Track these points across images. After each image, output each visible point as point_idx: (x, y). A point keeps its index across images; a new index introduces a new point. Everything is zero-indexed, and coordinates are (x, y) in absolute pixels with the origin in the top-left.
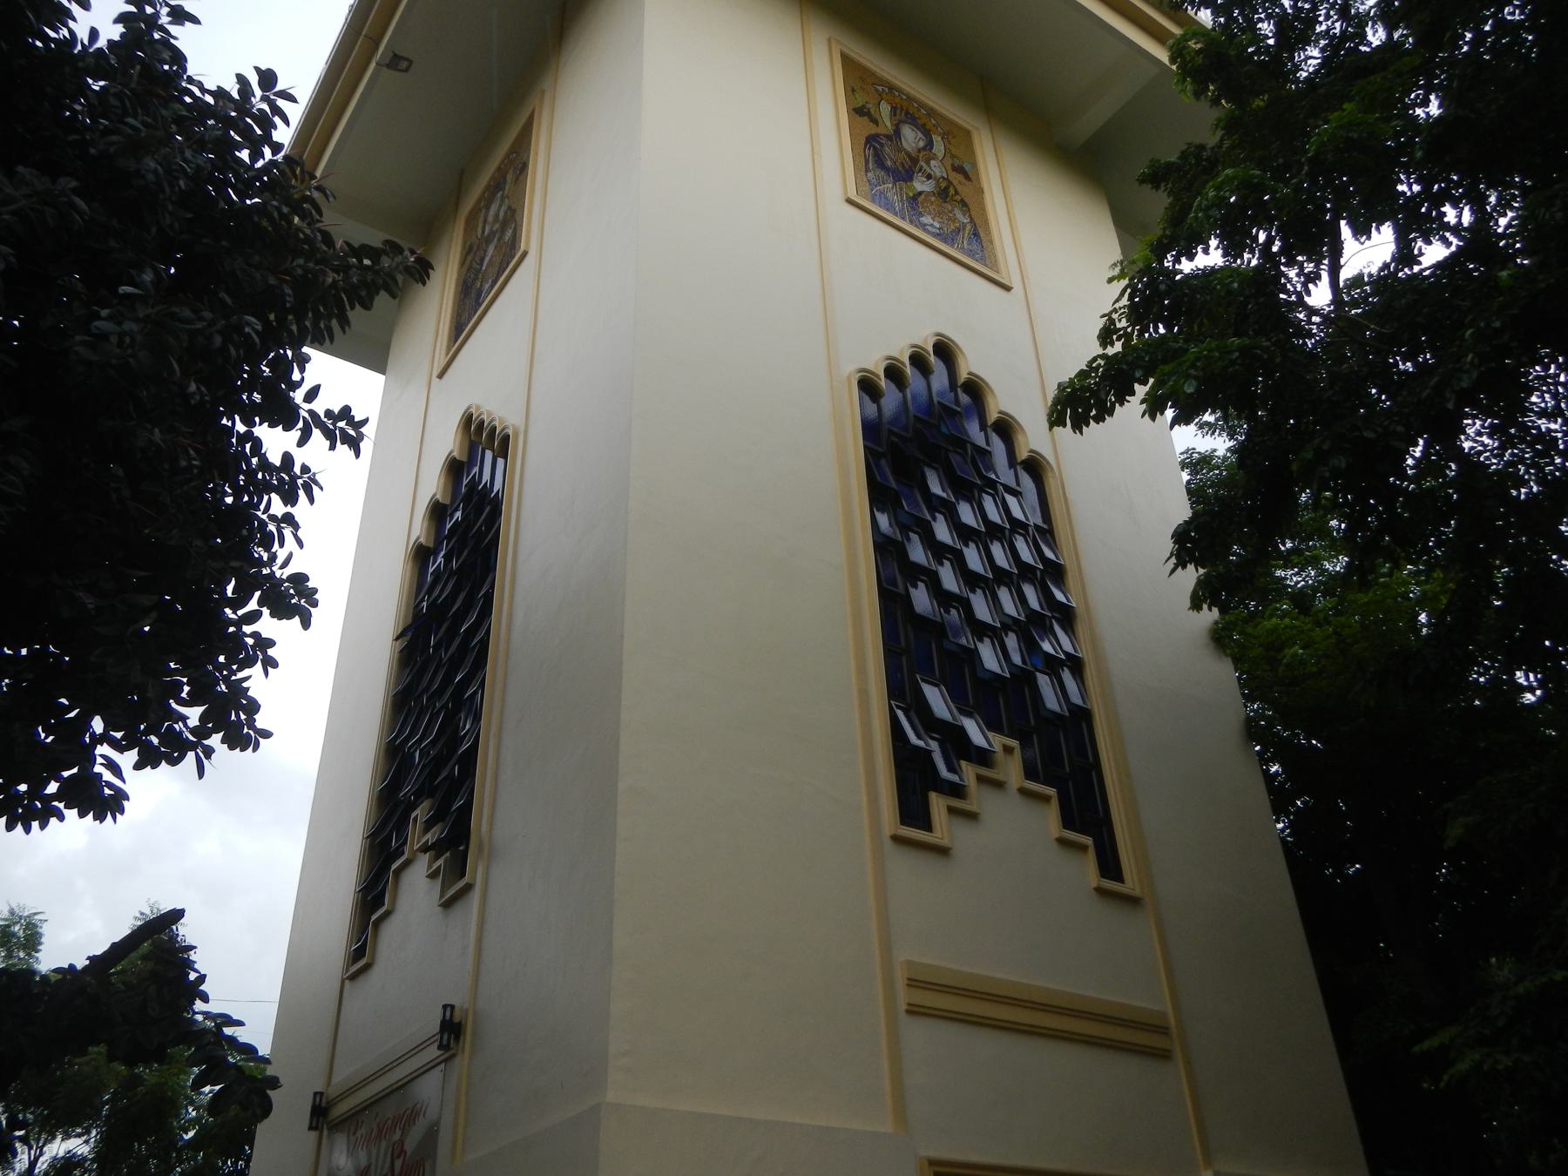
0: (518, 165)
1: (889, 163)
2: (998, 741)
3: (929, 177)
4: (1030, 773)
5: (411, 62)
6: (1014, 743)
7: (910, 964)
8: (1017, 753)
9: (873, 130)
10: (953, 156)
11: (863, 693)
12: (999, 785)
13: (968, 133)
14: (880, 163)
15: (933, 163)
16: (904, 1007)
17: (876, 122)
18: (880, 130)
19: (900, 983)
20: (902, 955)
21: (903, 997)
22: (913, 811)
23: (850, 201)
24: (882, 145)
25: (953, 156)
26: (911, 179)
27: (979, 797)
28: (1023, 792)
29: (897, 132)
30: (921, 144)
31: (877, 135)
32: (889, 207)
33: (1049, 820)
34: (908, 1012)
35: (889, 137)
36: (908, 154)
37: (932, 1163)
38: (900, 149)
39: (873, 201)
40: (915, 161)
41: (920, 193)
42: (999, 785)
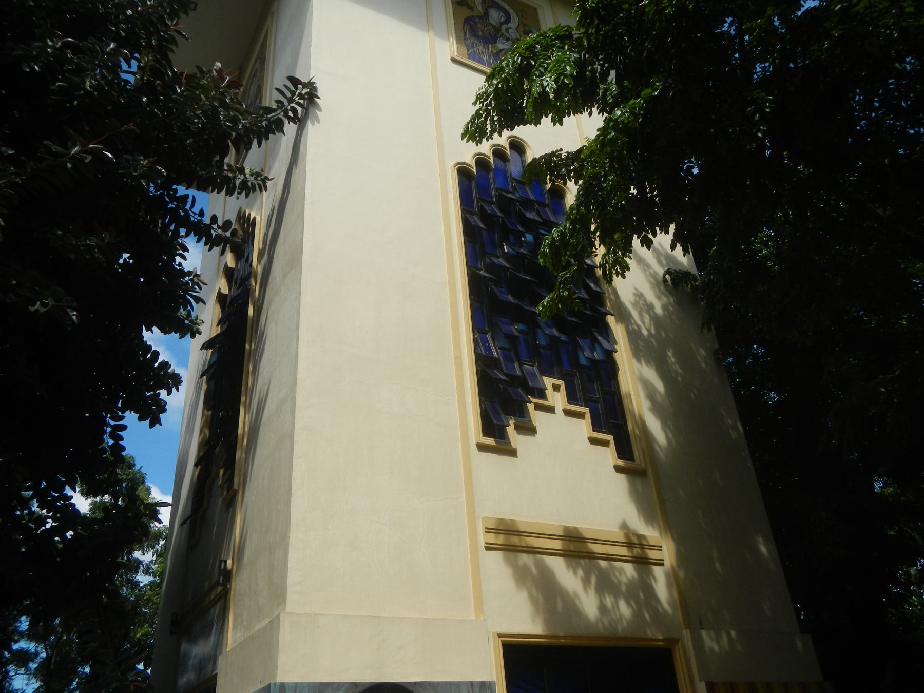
0: (262, 59)
1: (480, 33)
2: (548, 382)
3: (508, 39)
4: (571, 398)
5: (196, 4)
6: (561, 383)
7: (484, 519)
8: (563, 388)
9: (469, 13)
10: (524, 25)
11: (459, 359)
12: (551, 410)
14: (474, 34)
15: (510, 31)
16: (483, 545)
17: (471, 8)
18: (475, 13)
21: (483, 538)
22: (492, 427)
23: (454, 60)
24: (475, 22)
25: (524, 25)
26: (495, 42)
27: (538, 418)
28: (567, 413)
29: (486, 13)
30: (503, 19)
31: (473, 17)
32: (480, 61)
33: (583, 427)
34: (487, 549)
35: (480, 17)
36: (494, 27)
37: (500, 636)
38: (489, 24)
39: (469, 58)
40: (497, 30)
41: (502, 50)
42: (551, 410)
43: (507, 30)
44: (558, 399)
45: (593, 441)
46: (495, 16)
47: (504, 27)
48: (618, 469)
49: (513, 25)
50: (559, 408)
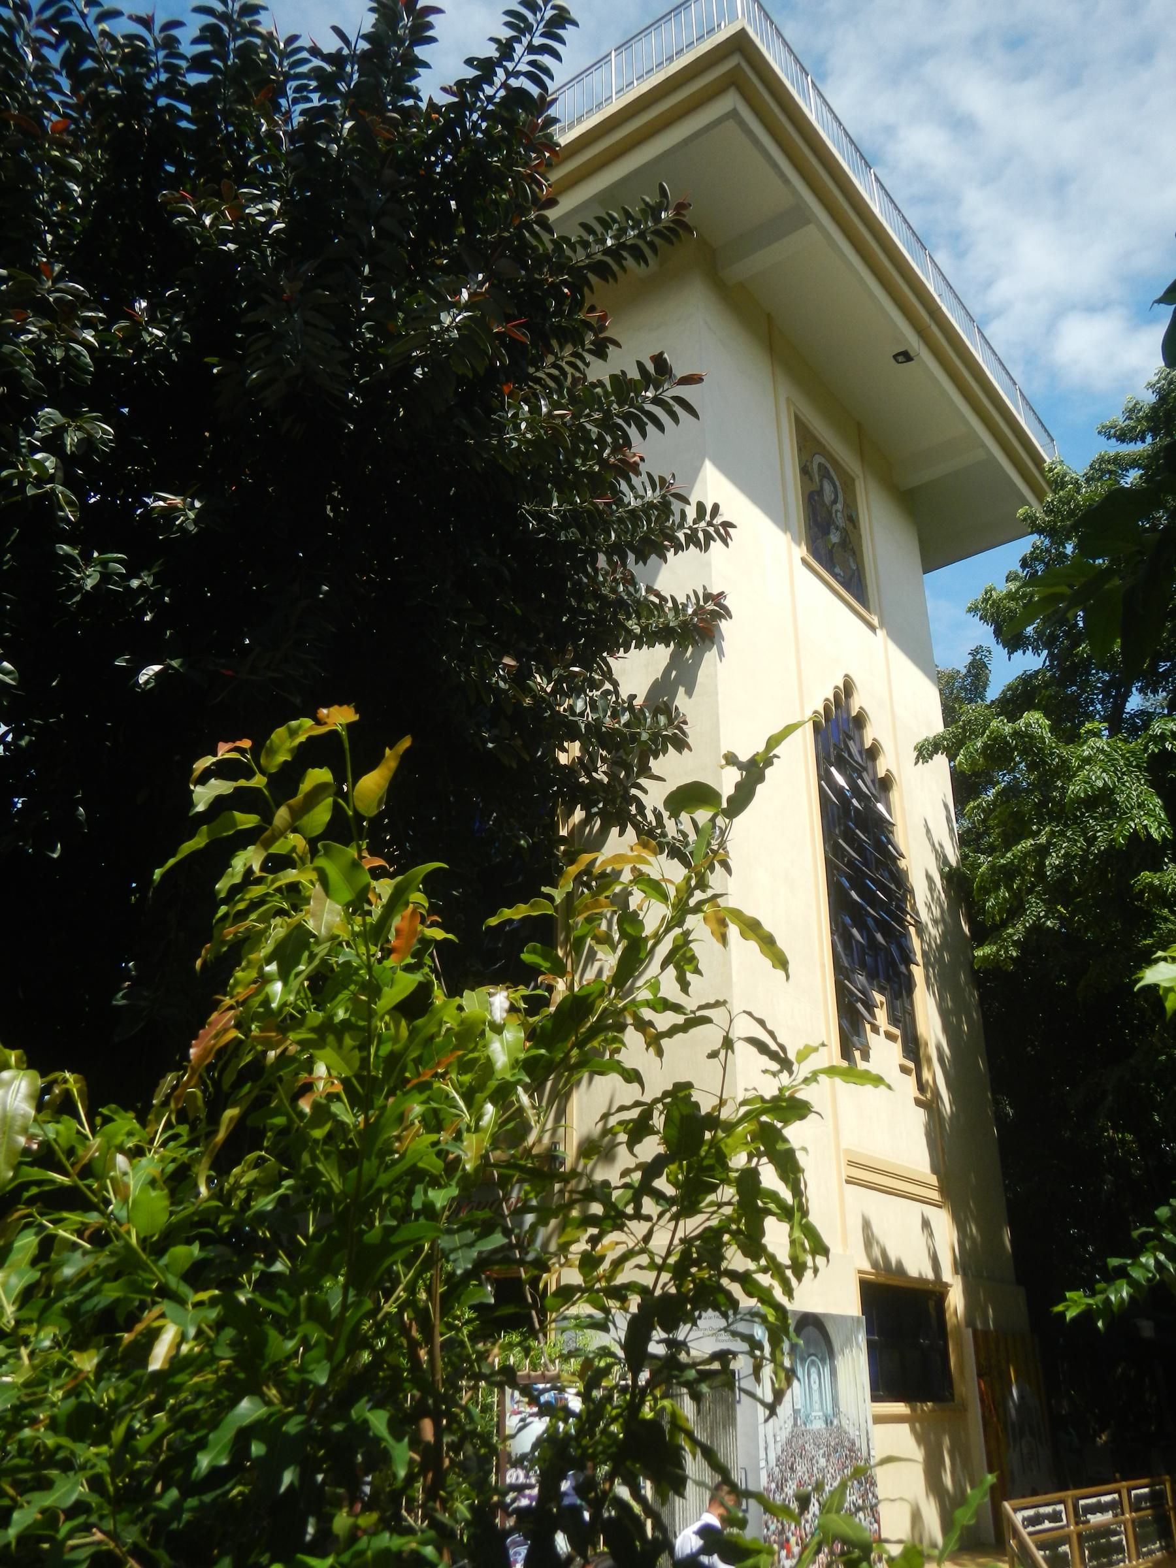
2: (878, 998)
3: (837, 529)
6: (883, 999)
7: (847, 1151)
11: (823, 965)
12: (875, 1029)
13: (853, 480)
16: (844, 1177)
19: (843, 1163)
20: (843, 1146)
23: (804, 561)
26: (828, 533)
28: (890, 1036)
34: (848, 1182)
37: (860, 1272)
40: (830, 513)
42: (875, 1029)
43: (837, 511)
44: (881, 1016)
45: (904, 1070)
46: (828, 494)
47: (835, 508)
48: (918, 1103)
49: (839, 506)
50: (882, 1031)
